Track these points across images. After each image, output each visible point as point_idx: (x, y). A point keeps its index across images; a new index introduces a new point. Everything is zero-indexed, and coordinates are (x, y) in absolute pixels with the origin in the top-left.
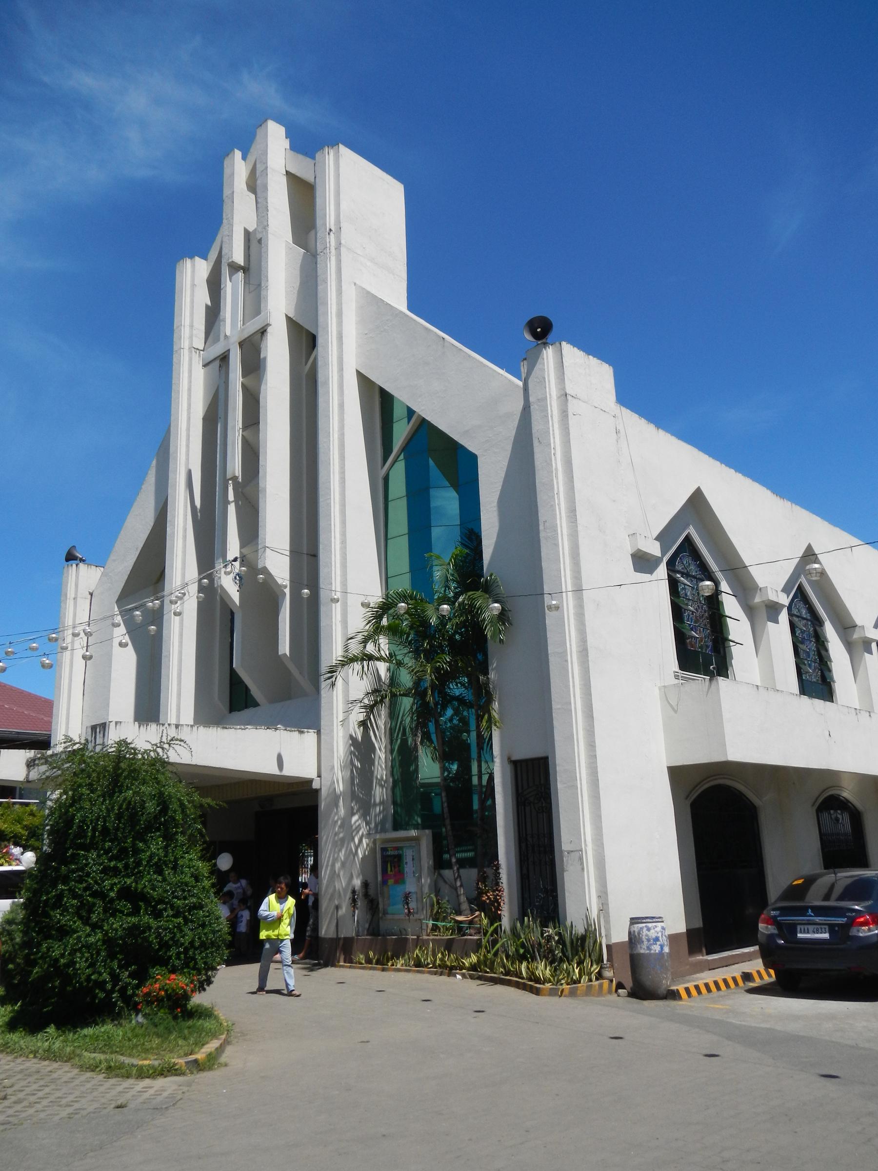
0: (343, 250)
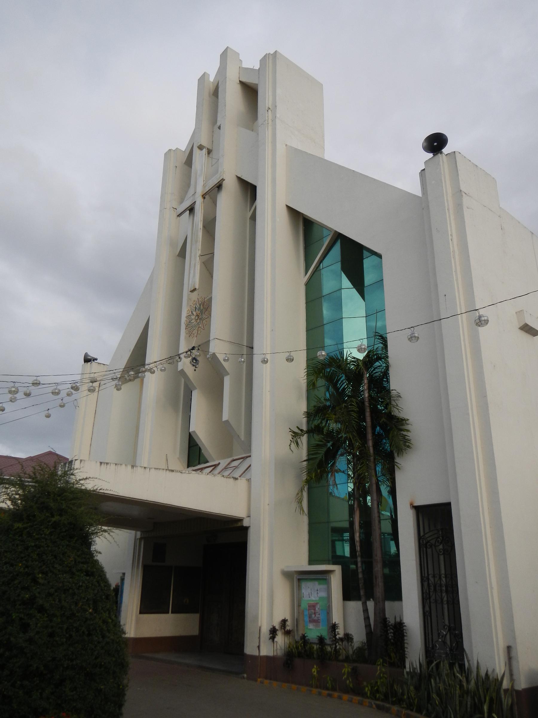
0: (278, 121)
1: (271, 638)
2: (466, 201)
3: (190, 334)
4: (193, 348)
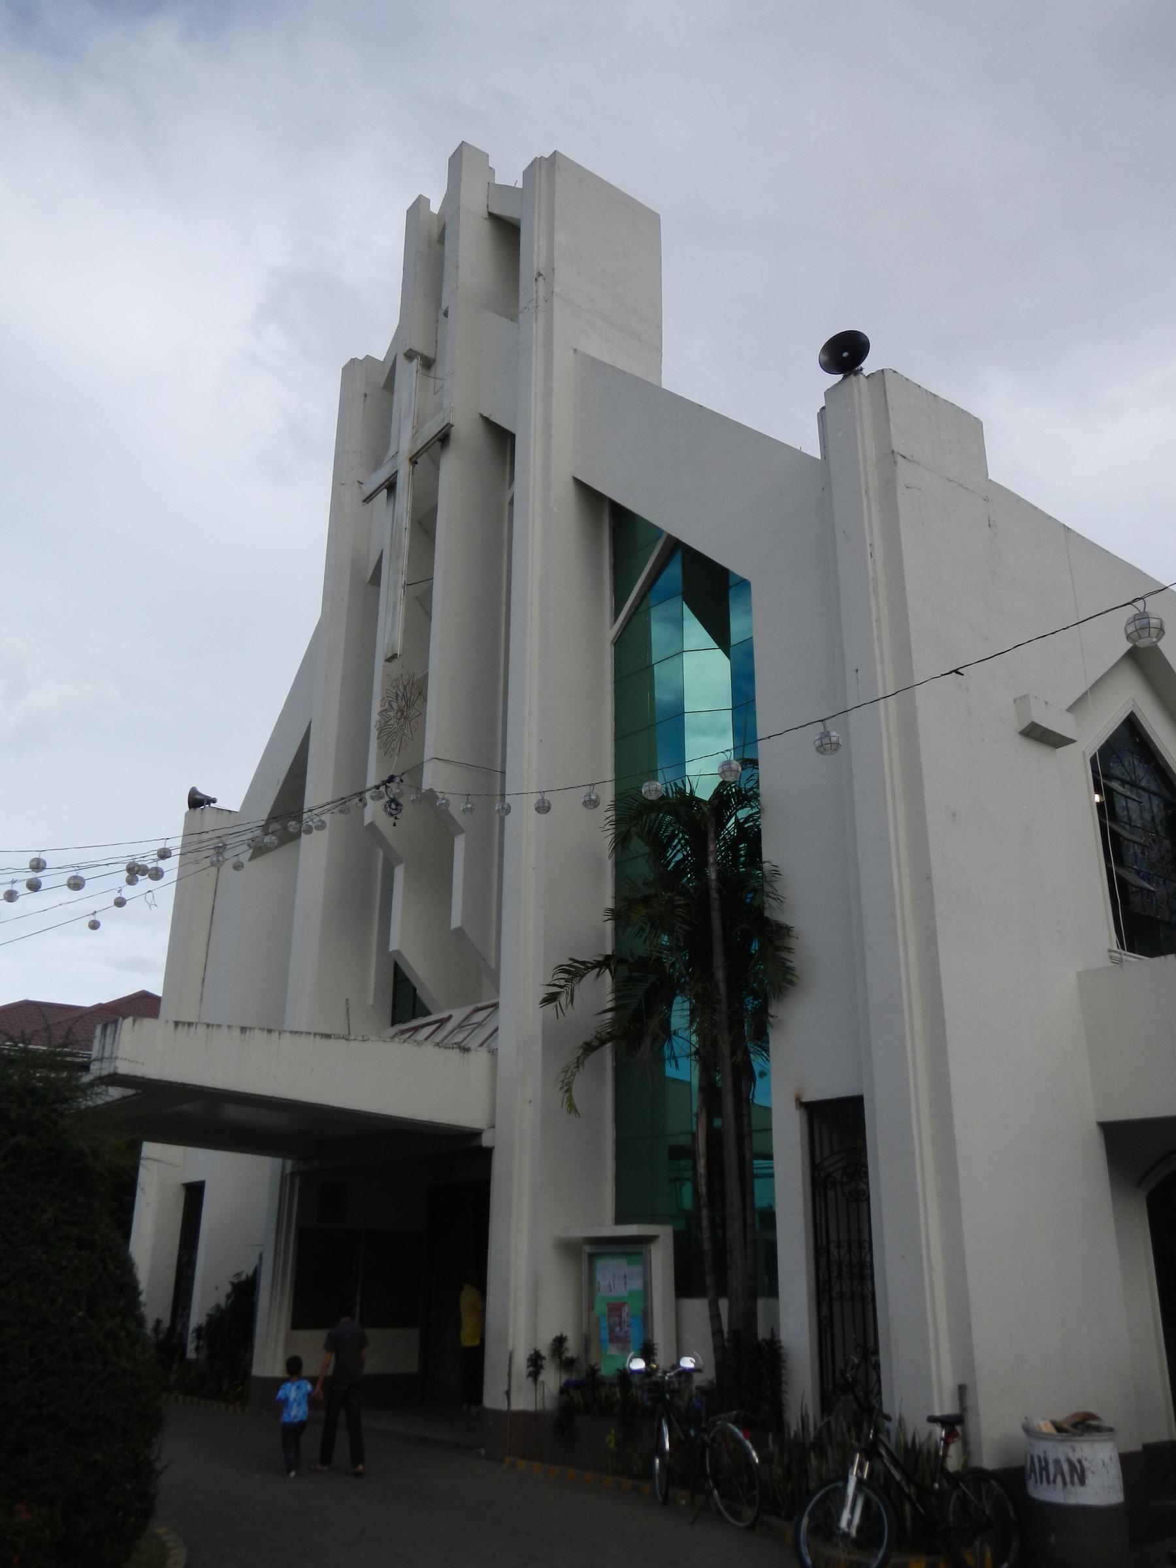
0: (557, 303)
1: (529, 1375)
2: (904, 472)
3: (386, 748)
4: (391, 779)
